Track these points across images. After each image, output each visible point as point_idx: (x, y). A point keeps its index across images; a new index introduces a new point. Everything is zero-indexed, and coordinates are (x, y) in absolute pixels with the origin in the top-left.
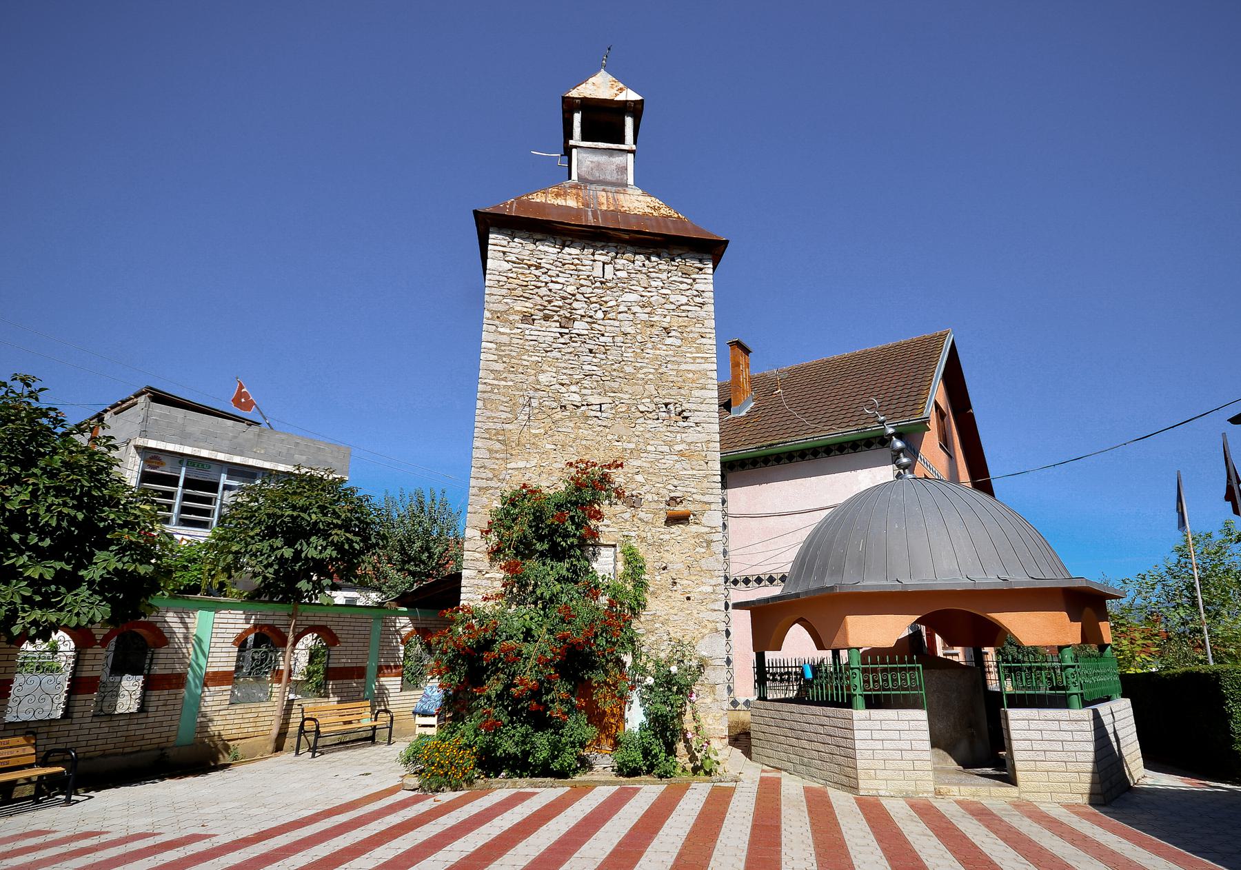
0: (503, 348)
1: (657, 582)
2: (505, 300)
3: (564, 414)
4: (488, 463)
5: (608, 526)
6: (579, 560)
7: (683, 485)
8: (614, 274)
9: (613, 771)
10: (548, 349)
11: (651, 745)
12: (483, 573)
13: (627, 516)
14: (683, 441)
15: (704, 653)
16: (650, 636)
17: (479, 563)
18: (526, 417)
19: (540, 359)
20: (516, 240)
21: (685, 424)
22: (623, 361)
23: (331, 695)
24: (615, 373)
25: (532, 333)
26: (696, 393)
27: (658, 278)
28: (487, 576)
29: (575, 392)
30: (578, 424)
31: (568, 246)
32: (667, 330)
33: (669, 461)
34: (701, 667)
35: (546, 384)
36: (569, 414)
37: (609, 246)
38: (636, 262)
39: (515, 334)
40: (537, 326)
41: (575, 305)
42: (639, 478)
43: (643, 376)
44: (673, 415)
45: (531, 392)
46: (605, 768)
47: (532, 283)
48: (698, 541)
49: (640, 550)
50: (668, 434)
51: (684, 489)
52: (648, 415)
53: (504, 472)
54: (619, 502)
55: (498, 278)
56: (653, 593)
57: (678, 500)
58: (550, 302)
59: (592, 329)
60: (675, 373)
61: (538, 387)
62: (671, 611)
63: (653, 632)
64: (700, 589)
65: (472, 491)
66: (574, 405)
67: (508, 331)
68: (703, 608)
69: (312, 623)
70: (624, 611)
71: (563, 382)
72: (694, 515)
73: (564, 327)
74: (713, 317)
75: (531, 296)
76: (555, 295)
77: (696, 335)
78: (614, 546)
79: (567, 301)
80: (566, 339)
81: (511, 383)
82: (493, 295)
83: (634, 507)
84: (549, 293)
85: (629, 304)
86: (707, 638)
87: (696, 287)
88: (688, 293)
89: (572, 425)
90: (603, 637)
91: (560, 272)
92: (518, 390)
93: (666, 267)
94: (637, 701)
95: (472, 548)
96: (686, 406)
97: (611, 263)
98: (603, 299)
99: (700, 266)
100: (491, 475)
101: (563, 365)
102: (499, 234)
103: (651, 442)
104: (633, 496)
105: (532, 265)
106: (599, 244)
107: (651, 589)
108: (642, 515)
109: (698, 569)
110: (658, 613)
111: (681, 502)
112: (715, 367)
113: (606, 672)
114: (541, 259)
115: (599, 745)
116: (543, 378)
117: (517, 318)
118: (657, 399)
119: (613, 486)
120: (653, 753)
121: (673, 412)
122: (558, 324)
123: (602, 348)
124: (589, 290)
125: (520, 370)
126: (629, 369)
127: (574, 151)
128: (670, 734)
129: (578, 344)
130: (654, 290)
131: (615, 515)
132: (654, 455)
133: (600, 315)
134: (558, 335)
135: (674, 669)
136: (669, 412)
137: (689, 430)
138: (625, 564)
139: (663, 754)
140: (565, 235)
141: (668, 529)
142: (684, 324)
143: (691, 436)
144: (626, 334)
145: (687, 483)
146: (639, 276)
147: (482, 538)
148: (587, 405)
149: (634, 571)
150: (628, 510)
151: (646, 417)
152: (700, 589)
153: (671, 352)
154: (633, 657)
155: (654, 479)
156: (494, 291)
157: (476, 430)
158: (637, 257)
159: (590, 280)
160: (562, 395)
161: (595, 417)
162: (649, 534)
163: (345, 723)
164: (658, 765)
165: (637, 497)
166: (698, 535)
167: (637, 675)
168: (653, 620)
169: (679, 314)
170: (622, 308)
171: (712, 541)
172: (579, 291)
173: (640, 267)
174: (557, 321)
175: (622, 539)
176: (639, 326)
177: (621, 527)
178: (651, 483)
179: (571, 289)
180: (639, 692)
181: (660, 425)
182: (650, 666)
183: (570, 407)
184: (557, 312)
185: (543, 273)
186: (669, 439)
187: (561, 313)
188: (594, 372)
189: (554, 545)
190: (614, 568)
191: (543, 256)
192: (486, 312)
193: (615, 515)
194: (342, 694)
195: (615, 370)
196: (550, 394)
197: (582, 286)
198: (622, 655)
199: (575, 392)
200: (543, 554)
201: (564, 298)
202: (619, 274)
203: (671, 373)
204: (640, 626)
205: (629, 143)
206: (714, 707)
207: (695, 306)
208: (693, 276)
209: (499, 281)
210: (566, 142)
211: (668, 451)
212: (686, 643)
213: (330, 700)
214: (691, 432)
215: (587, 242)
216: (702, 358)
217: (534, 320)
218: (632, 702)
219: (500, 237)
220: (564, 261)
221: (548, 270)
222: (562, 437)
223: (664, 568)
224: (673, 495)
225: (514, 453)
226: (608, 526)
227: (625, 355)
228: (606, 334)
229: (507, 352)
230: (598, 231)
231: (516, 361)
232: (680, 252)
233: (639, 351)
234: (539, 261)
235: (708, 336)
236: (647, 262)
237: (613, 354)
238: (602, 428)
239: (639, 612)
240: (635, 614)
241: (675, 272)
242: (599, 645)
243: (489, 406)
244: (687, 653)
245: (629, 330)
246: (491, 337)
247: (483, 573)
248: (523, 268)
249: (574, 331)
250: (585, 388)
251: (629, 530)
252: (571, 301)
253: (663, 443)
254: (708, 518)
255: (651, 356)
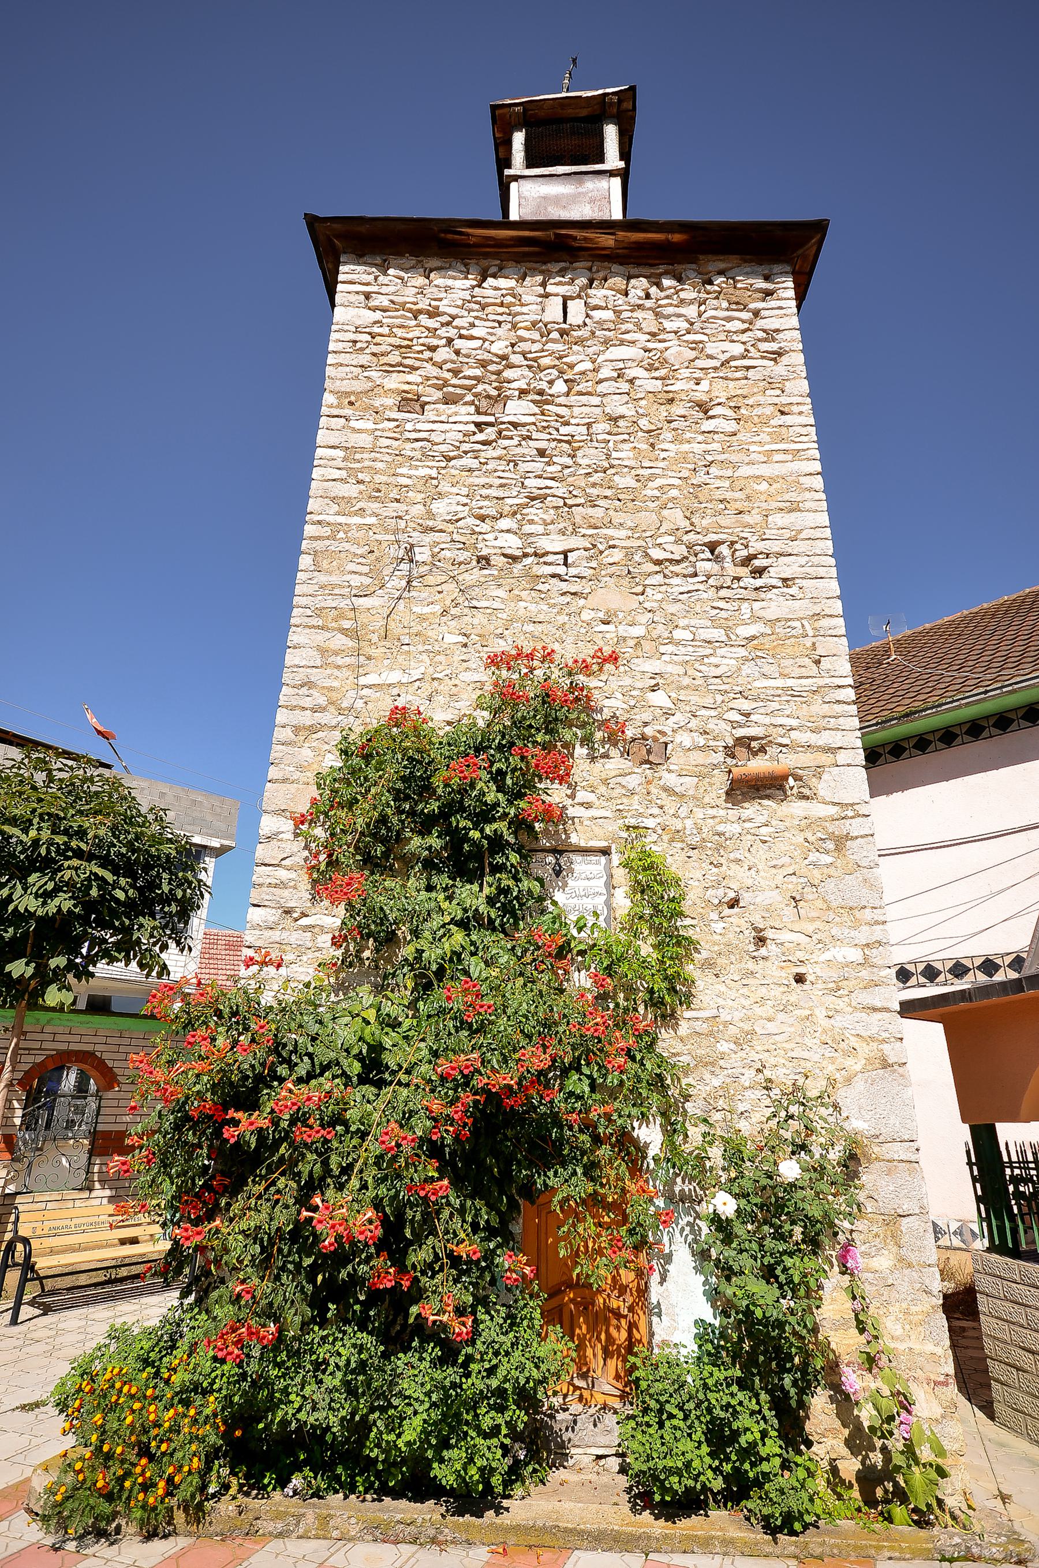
0: (358, 456)
1: (717, 937)
2: (366, 374)
3: (485, 572)
4: (315, 675)
5: (588, 805)
6: (517, 880)
7: (762, 710)
8: (588, 316)
9: (623, 1470)
10: (451, 454)
11: (735, 1414)
12: (295, 915)
13: (632, 782)
14: (756, 619)
15: (858, 1124)
16: (707, 1076)
17: (286, 893)
18: (404, 583)
19: (434, 473)
20: (391, 271)
21: (759, 583)
22: (612, 466)
23: (97, 1185)
24: (594, 492)
25: (419, 426)
26: (778, 519)
27: (679, 316)
28: (304, 921)
29: (508, 531)
30: (516, 592)
31: (494, 276)
32: (703, 408)
33: (727, 660)
34: (852, 1162)
35: (449, 517)
36: (496, 573)
37: (575, 269)
38: (632, 293)
39: (383, 430)
40: (430, 413)
41: (508, 374)
42: (659, 698)
43: (657, 493)
44: (728, 564)
45: (415, 534)
46: (599, 1457)
47: (421, 341)
48: (811, 839)
49: (669, 860)
50: (721, 604)
51: (767, 720)
52: (672, 568)
53: (352, 694)
54: (614, 752)
55: (352, 336)
56: (708, 965)
57: (754, 744)
58: (456, 373)
59: (543, 414)
60: (727, 484)
61: (431, 523)
62: (759, 1011)
63: (713, 1064)
64: (827, 955)
65: (279, 734)
66: (505, 555)
67: (370, 425)
68: (840, 1004)
69: (63, 1047)
70: (635, 1010)
71: (482, 511)
72: (798, 778)
73: (486, 414)
74: (804, 374)
75: (417, 364)
76: (466, 360)
77: (769, 410)
78: (605, 852)
79: (492, 368)
80: (490, 433)
81: (373, 520)
82: (341, 365)
83: (651, 763)
84: (454, 357)
85: (621, 365)
86: (859, 1083)
87: (760, 323)
88: (744, 337)
89: (501, 593)
90: (582, 1074)
91: (476, 318)
92: (386, 531)
93: (694, 295)
94: (683, 1259)
95: (274, 858)
96: (756, 546)
97: (579, 296)
98: (565, 360)
99: (770, 286)
100: (322, 701)
101: (482, 481)
102: (359, 264)
103: (682, 623)
104: (644, 738)
105: (420, 312)
106: (555, 267)
107: (705, 954)
108: (671, 779)
109: (819, 903)
110: (725, 1016)
111: (762, 750)
112: (817, 466)
113: (591, 1170)
114: (440, 300)
115: (584, 1376)
116: (440, 507)
117: (390, 401)
118: (692, 537)
119: (599, 717)
120: (743, 1440)
121: (729, 559)
122: (472, 409)
123: (565, 446)
124: (537, 347)
125: (394, 494)
126: (625, 481)
127: (513, 186)
128: (795, 1383)
129: (515, 442)
130: (672, 336)
131: (605, 782)
132: (691, 649)
133: (560, 387)
134: (472, 428)
135: (790, 1170)
136: (718, 559)
137: (769, 595)
138: (634, 892)
139: (772, 1447)
140: (486, 256)
141: (733, 813)
142: (739, 392)
143: (775, 606)
144: (615, 419)
145: (775, 706)
146: (639, 314)
147: (296, 835)
148: (536, 554)
149: (655, 908)
150: (636, 770)
151: (666, 572)
152: (827, 955)
153: (716, 446)
154: (665, 1131)
155: (695, 698)
156: (342, 358)
157: (296, 612)
158: (633, 281)
159: (540, 328)
160: (480, 537)
161: (553, 576)
162: (689, 823)
163: (123, 1242)
164: (761, 1486)
165: (655, 740)
166: (809, 823)
167: (679, 1180)
168: (711, 1034)
169: (730, 375)
170: (606, 372)
171: (848, 837)
172: (516, 349)
173: (640, 298)
174: (472, 403)
175: (625, 835)
176: (643, 403)
177: (621, 807)
178: (688, 709)
179: (499, 347)
180: (688, 1229)
181: (701, 587)
182: (716, 1153)
183: (499, 561)
184: (469, 389)
185: (443, 325)
186: (723, 615)
187: (480, 388)
188: (548, 491)
189: (456, 839)
190: (608, 904)
191: (443, 295)
192: (326, 395)
193: (605, 782)
194: (120, 1184)
195: (594, 485)
196: (456, 537)
197: (522, 339)
198: (636, 1124)
199: (508, 531)
200: (430, 865)
201: (483, 364)
202: (597, 314)
203: (718, 483)
204: (679, 1047)
205: (613, 159)
206: (905, 1282)
207: (763, 358)
208: (752, 306)
209: (355, 342)
210: (500, 173)
211: (724, 638)
212: (813, 1093)
213: (94, 1194)
214: (774, 597)
215: (529, 265)
216: (785, 451)
217: (423, 407)
218: (668, 1258)
219: (359, 268)
220: (483, 301)
221: (454, 317)
222: (479, 618)
223: (733, 904)
224: (740, 732)
225: (372, 651)
226: (588, 805)
227: (615, 455)
228: (573, 421)
229: (367, 463)
230: (551, 234)
231: (384, 479)
232: (722, 266)
233: (644, 446)
234: (433, 303)
235: (795, 409)
236: (653, 290)
237: (588, 457)
238: (568, 598)
239: (673, 1011)
240: (669, 1018)
241: (715, 302)
242: (571, 1094)
243: (325, 564)
244: (818, 1125)
245: (622, 410)
246: (333, 438)
247: (295, 915)
248: (403, 317)
249: (506, 419)
250: (531, 522)
251: (641, 815)
252: (501, 367)
253: (709, 623)
254: (833, 784)
255: (672, 454)
